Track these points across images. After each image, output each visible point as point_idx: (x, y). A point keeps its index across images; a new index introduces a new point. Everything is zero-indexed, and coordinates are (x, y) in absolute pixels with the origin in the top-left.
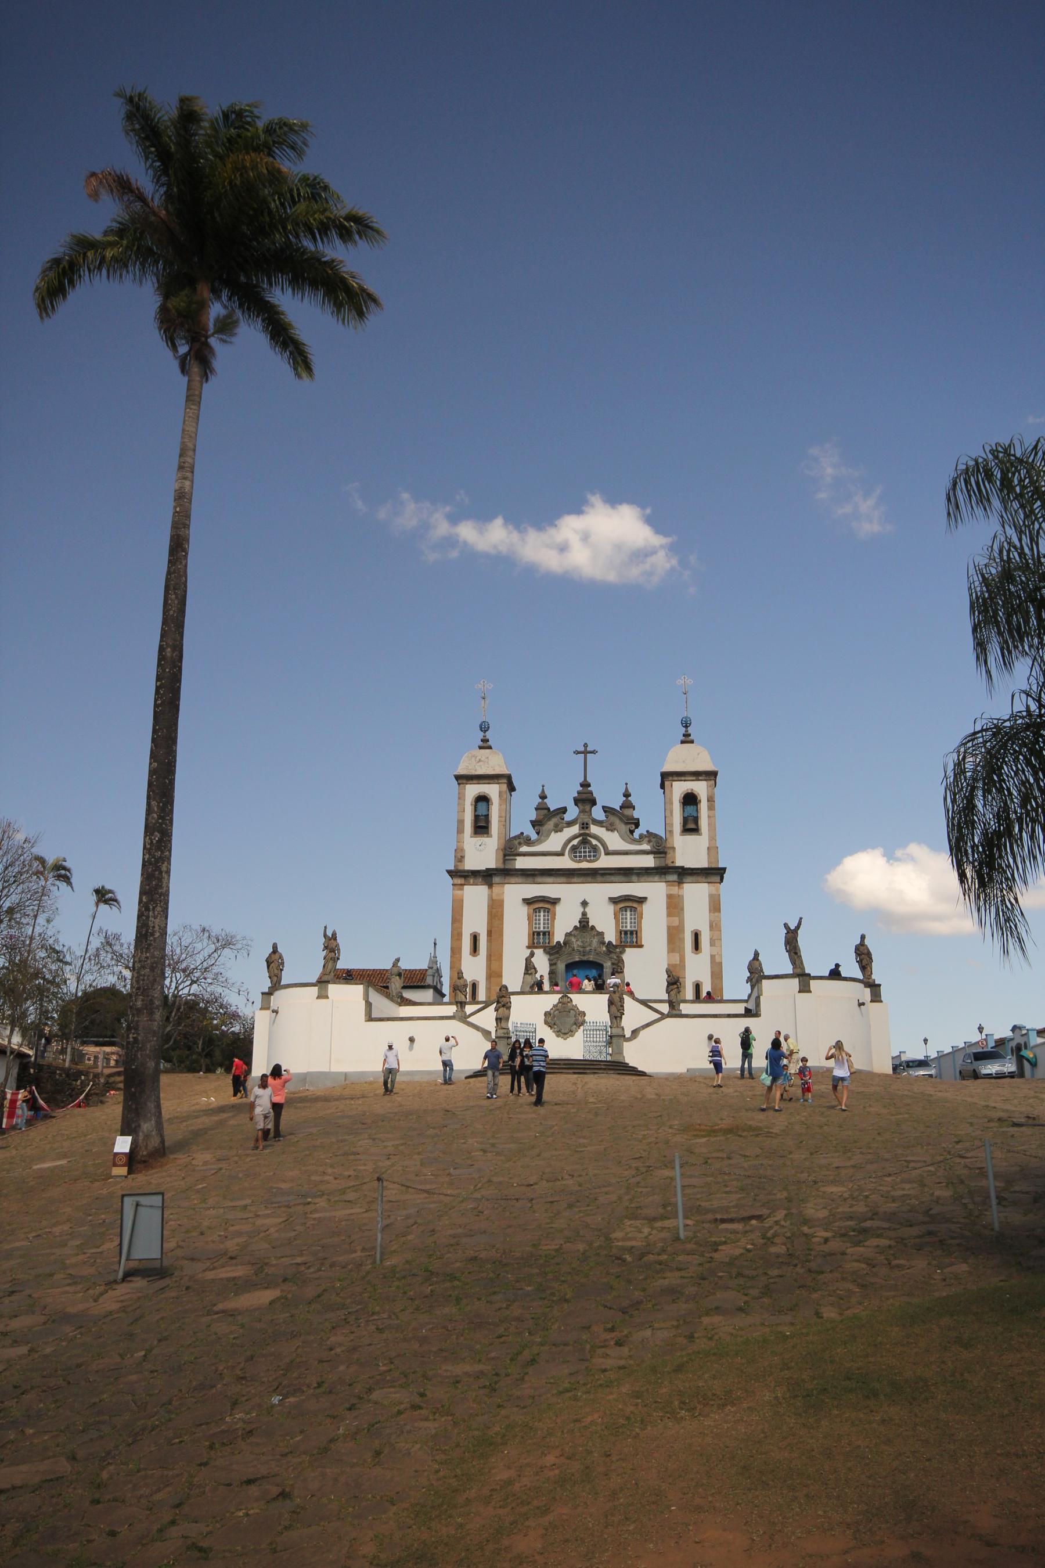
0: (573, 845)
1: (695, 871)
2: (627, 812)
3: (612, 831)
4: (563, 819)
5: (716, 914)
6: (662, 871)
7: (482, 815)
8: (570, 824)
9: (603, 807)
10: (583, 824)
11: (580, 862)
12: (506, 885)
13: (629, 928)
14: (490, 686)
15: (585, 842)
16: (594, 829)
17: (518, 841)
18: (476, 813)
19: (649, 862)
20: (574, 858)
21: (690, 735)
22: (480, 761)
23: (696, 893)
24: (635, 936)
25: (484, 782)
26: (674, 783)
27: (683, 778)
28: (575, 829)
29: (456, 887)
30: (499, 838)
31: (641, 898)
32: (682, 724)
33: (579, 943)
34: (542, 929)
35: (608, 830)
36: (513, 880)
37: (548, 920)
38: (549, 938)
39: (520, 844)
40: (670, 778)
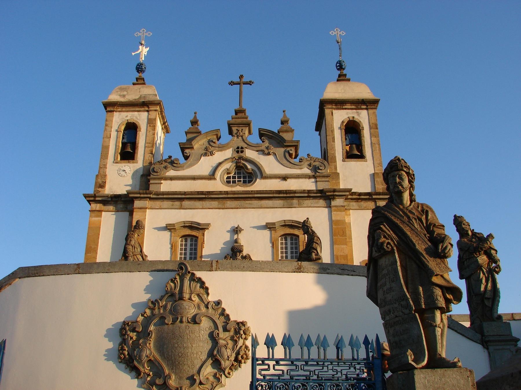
1: (362, 197)
2: (286, 136)
3: (269, 154)
8: (222, 148)
9: (260, 130)
10: (238, 148)
11: (232, 186)
14: (149, 34)
15: (240, 168)
16: (250, 154)
21: (345, 75)
26: (335, 112)
29: (93, 214)
32: (337, 66)
36: (158, 203)
39: (166, 168)
40: (330, 106)
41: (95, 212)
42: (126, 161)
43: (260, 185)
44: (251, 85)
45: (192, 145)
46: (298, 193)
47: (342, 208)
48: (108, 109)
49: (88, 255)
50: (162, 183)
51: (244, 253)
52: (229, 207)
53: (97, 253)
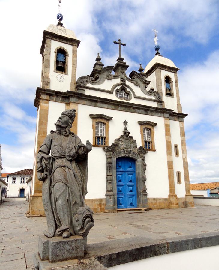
0: (117, 89)
1: (175, 114)
3: (137, 86)
4: (111, 73)
5: (184, 137)
6: (162, 111)
7: (61, 61)
8: (115, 77)
10: (122, 79)
11: (121, 99)
12: (80, 105)
13: (146, 140)
16: (128, 83)
17: (86, 80)
18: (58, 59)
19: (155, 105)
20: (117, 96)
21: (159, 53)
22: (60, 29)
23: (175, 125)
24: (150, 144)
25: (63, 41)
26: (162, 71)
27: (164, 69)
28: (118, 81)
30: (72, 77)
31: (154, 123)
33: (125, 146)
34: (100, 135)
35: (135, 85)
37: (103, 130)
38: (105, 141)
39: (87, 82)
40: (160, 67)
41: (44, 100)
42: (61, 72)
43: (133, 101)
44: (124, 46)
45: (101, 72)
46: (151, 108)
47: (169, 119)
48: (47, 36)
49: (41, 126)
50: (85, 90)
51: (130, 135)
52: (120, 110)
53: (47, 126)
